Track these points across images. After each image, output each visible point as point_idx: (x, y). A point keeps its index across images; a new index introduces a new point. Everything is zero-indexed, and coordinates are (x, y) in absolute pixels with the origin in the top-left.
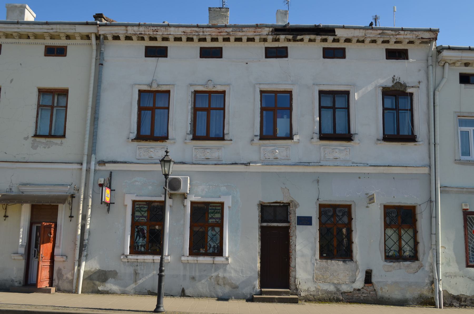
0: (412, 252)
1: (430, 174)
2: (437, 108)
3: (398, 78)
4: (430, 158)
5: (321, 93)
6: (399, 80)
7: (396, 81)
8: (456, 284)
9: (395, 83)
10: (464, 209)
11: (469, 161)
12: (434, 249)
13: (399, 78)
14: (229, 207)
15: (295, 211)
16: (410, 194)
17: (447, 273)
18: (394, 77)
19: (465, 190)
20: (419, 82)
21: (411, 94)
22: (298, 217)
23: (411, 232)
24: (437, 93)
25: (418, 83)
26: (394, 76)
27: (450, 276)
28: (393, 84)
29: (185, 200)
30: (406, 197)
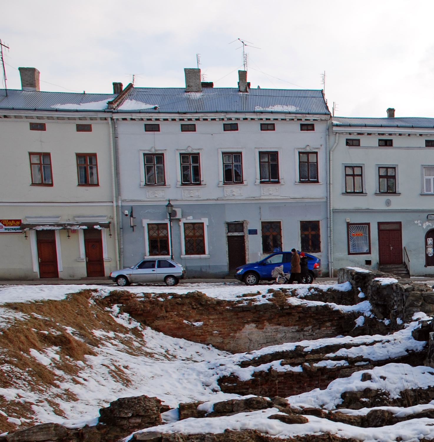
1: (327, 202)
2: (331, 162)
4: (327, 192)
5: (261, 153)
14: (207, 226)
15: (247, 227)
20: (321, 145)
22: (249, 230)
24: (331, 152)
29: (180, 222)
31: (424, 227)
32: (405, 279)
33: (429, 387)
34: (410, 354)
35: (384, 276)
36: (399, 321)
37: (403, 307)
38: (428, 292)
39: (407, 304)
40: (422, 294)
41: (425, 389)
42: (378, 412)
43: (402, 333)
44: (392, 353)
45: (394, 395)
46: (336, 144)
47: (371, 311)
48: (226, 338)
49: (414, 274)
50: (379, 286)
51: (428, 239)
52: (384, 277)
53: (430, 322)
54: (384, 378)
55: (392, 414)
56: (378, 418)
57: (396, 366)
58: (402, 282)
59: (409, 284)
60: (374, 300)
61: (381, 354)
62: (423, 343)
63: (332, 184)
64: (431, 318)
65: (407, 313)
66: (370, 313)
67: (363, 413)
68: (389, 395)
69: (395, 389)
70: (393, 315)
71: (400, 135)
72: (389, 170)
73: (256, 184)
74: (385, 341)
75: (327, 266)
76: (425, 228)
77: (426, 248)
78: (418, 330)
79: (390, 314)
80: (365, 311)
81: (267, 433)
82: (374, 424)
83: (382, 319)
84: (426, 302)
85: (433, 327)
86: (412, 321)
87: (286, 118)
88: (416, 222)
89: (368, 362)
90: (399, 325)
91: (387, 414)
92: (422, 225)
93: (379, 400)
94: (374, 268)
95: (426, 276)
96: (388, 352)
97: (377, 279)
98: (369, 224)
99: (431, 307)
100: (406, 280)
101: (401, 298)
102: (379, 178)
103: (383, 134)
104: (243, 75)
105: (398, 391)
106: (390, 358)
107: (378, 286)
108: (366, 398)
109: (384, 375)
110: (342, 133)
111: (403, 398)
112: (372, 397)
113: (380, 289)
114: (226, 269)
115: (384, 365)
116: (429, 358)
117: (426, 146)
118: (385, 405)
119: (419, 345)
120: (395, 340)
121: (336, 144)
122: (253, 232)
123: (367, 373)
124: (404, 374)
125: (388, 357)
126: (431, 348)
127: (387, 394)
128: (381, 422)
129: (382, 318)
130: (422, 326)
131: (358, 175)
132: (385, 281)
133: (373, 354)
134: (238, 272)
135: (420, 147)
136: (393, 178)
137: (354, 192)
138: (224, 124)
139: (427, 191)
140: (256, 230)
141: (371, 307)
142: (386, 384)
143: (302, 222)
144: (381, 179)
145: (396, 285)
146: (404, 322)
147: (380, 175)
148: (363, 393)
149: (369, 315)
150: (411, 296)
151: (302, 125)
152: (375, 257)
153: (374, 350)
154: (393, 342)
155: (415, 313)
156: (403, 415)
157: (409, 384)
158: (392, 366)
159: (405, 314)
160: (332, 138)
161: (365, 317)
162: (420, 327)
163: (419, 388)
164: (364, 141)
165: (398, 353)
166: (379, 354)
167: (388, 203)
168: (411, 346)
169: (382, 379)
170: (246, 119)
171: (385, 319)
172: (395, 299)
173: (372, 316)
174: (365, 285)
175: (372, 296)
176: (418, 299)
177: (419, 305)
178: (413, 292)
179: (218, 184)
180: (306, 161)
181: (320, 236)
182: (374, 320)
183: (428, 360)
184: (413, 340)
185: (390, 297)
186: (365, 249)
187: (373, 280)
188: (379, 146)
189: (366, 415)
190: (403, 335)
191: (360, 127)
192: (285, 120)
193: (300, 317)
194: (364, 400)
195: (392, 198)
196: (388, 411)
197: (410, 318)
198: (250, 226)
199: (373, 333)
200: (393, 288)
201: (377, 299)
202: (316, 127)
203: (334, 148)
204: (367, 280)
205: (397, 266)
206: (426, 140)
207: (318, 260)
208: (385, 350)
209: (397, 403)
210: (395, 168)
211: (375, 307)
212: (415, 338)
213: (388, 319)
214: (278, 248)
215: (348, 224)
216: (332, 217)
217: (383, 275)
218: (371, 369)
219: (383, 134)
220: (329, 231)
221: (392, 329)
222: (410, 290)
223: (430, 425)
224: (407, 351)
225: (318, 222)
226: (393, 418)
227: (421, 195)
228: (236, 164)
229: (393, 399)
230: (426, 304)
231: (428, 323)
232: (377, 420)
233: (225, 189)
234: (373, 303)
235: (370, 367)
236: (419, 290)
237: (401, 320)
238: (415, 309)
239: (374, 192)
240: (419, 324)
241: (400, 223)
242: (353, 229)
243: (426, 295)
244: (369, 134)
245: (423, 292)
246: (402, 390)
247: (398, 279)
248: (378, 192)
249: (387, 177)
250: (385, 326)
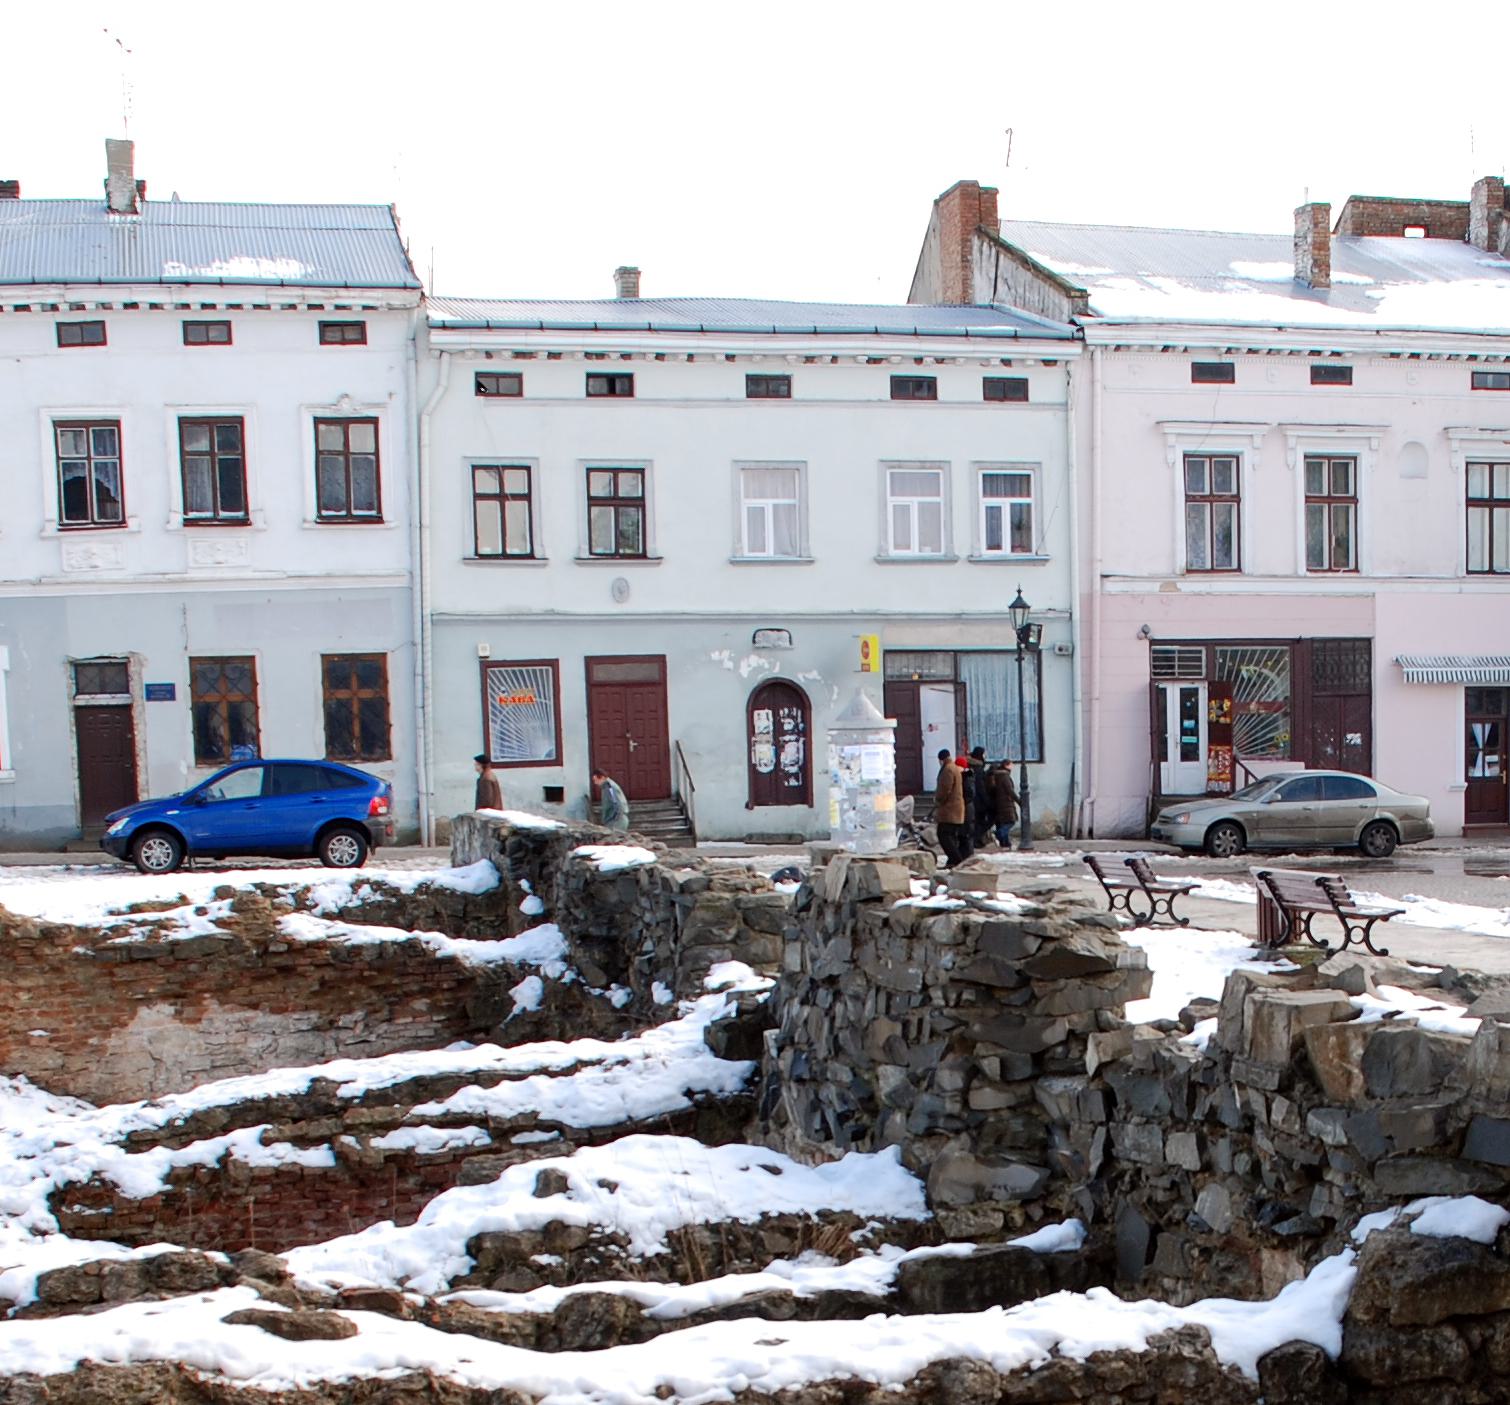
2: (425, 452)
4: (411, 554)
5: (185, 423)
20: (391, 395)
24: (425, 419)
31: (744, 671)
32: (679, 850)
33: (764, 1214)
34: (697, 1104)
35: (609, 839)
36: (660, 994)
37: (672, 945)
38: (760, 894)
39: (686, 936)
40: (737, 902)
41: (750, 1222)
42: (593, 1300)
43: (672, 1033)
44: (636, 1101)
45: (645, 1242)
46: (441, 390)
47: (565, 958)
48: (72, 1052)
49: (709, 833)
50: (592, 874)
51: (756, 712)
52: (607, 844)
53: (767, 995)
54: (611, 1187)
55: (640, 1306)
56: (593, 1319)
57: (652, 1146)
58: (670, 859)
59: (693, 868)
60: (576, 921)
61: (600, 1104)
62: (743, 1066)
64: (770, 983)
65: (689, 965)
66: (561, 966)
67: (543, 1305)
68: (630, 1242)
69: (650, 1223)
70: (641, 972)
71: (660, 357)
72: (621, 476)
73: (169, 527)
74: (613, 1060)
75: (412, 808)
77: (751, 745)
78: (726, 1022)
79: (631, 970)
80: (543, 958)
81: (219, 1371)
82: (578, 1341)
83: (602, 988)
84: (752, 928)
85: (775, 1011)
86: (705, 991)
87: (270, 301)
88: (715, 656)
89: (555, 1133)
90: (660, 1007)
91: (621, 1309)
92: (737, 666)
93: (596, 1261)
94: (572, 814)
95: (749, 839)
96: (623, 1097)
97: (583, 850)
98: (554, 663)
99: (770, 947)
100: (684, 853)
101: (668, 915)
102: (589, 506)
103: (601, 356)
104: (120, 154)
105: (661, 1229)
106: (630, 1118)
107: (588, 875)
108: (551, 1253)
109: (612, 1177)
110: (463, 352)
111: (675, 1252)
112: (571, 1251)
113: (594, 886)
114: (71, 820)
115: (612, 1140)
116: (764, 1118)
117: (749, 396)
118: (617, 1276)
119: (727, 1075)
120: (647, 1057)
122: (162, 692)
123: (553, 1170)
124: (681, 1170)
125: (622, 1117)
126: (768, 1086)
127: (622, 1240)
128: (601, 1333)
129: (603, 981)
130: (740, 1012)
131: (516, 497)
132: (611, 857)
133: (575, 1106)
134: (113, 830)
135: (728, 400)
136: (637, 506)
137: (505, 556)
138: (59, 325)
139: (752, 550)
140: (173, 686)
141: (564, 947)
142: (618, 1207)
143: (327, 659)
144: (595, 510)
145: (651, 872)
146: (678, 997)
147: (593, 494)
148: (539, 1238)
149: (557, 975)
150: (702, 907)
151: (324, 326)
152: (575, 775)
153: (577, 1093)
154: (639, 1063)
155: (714, 966)
156: (677, 1312)
157: (696, 1206)
158: (637, 1145)
159: (680, 969)
160: (428, 367)
161: (545, 979)
162: (734, 1014)
163: (729, 1221)
164: (537, 378)
165: (658, 1102)
166: (592, 1106)
167: (620, 591)
168: (701, 1080)
169: (605, 1191)
170: (131, 306)
171: (613, 986)
172: (648, 917)
173: (569, 976)
174: (545, 872)
175: (567, 908)
176: (723, 918)
177: (729, 938)
178: (707, 894)
179: (42, 530)
180: (340, 448)
181: (388, 704)
182: (575, 991)
183: (762, 1124)
184: (709, 1058)
185: (628, 912)
186: (544, 749)
187: (571, 854)
188: (589, 395)
189: (550, 1309)
190: (675, 1038)
191: (523, 332)
192: (268, 307)
193: (323, 983)
194: (544, 1259)
195: (631, 572)
196: (624, 1298)
197: (697, 983)
198: (148, 673)
199: (570, 1034)
200: (638, 882)
201: (586, 918)
203: (433, 403)
204: (548, 853)
205: (650, 806)
206: (748, 377)
207: (382, 786)
208: (612, 1091)
209: (656, 1269)
210: (641, 471)
211: (579, 946)
212: (716, 1052)
213: (624, 984)
214: (244, 744)
215: (486, 665)
216: (428, 641)
217: (604, 836)
218: (568, 1154)
219: (601, 356)
220: (419, 686)
221: (638, 1021)
222: (695, 887)
223: (768, 1343)
224: (689, 1093)
225: (384, 655)
226: (643, 1320)
227: (733, 563)
228: (101, 459)
229: (642, 1255)
230: (752, 933)
231: (761, 998)
232: (590, 1329)
233: (65, 547)
234: (572, 933)
235: (563, 1148)
236: (727, 887)
237: (667, 988)
238: (714, 953)
239: (572, 554)
240: (728, 1002)
241: (660, 660)
243: (751, 905)
244: (554, 355)
245: (742, 895)
246: (673, 1227)
247: (655, 849)
248: (586, 555)
249: (614, 501)
250: (614, 1009)
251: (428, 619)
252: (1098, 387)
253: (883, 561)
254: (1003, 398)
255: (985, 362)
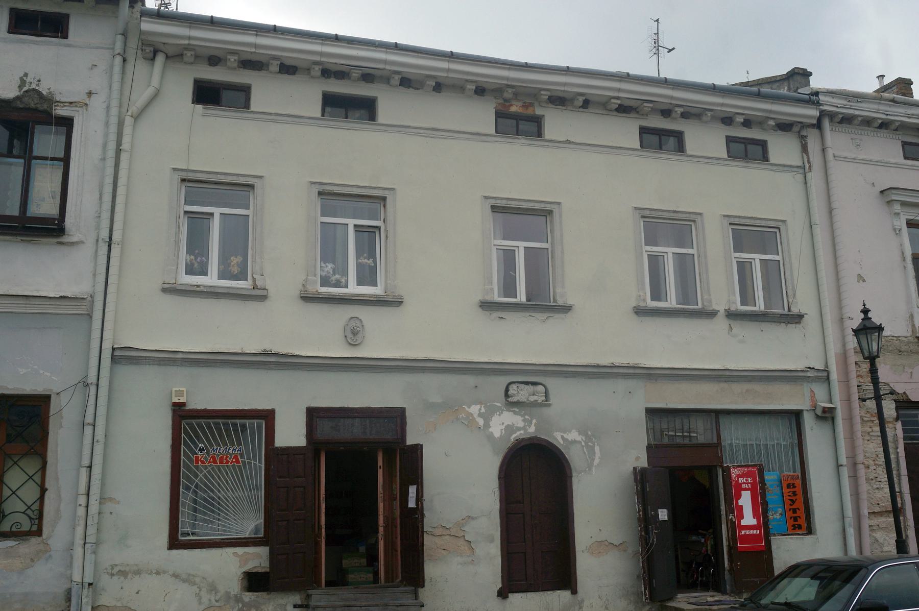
0: (27, 515)
2: (124, 157)
3: (36, 80)
6: (38, 85)
7: (30, 86)
8: (137, 593)
9: (26, 91)
10: (175, 405)
11: (198, 286)
12: (80, 505)
13: (39, 81)
16: (35, 367)
17: (116, 565)
18: (25, 78)
19: (180, 356)
20: (90, 94)
21: (67, 123)
23: (31, 466)
24: (128, 121)
25: (86, 96)
26: (26, 75)
27: (123, 574)
28: (19, 94)
30: (22, 373)
63: (122, 243)
71: (406, 82)
76: (497, 434)
92: (487, 425)
121: (150, 91)
202: (74, 27)
215: (180, 413)
216: (104, 382)
225: (48, 398)
242: (198, 437)
251: (107, 355)
252: (830, 153)
253: (641, 312)
254: (745, 157)
255: (727, 120)
